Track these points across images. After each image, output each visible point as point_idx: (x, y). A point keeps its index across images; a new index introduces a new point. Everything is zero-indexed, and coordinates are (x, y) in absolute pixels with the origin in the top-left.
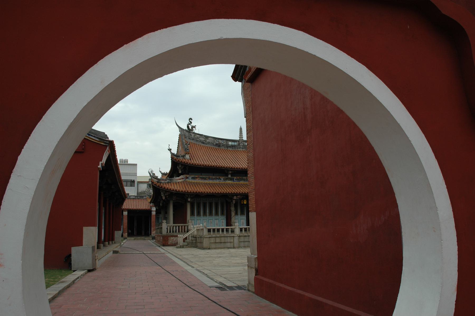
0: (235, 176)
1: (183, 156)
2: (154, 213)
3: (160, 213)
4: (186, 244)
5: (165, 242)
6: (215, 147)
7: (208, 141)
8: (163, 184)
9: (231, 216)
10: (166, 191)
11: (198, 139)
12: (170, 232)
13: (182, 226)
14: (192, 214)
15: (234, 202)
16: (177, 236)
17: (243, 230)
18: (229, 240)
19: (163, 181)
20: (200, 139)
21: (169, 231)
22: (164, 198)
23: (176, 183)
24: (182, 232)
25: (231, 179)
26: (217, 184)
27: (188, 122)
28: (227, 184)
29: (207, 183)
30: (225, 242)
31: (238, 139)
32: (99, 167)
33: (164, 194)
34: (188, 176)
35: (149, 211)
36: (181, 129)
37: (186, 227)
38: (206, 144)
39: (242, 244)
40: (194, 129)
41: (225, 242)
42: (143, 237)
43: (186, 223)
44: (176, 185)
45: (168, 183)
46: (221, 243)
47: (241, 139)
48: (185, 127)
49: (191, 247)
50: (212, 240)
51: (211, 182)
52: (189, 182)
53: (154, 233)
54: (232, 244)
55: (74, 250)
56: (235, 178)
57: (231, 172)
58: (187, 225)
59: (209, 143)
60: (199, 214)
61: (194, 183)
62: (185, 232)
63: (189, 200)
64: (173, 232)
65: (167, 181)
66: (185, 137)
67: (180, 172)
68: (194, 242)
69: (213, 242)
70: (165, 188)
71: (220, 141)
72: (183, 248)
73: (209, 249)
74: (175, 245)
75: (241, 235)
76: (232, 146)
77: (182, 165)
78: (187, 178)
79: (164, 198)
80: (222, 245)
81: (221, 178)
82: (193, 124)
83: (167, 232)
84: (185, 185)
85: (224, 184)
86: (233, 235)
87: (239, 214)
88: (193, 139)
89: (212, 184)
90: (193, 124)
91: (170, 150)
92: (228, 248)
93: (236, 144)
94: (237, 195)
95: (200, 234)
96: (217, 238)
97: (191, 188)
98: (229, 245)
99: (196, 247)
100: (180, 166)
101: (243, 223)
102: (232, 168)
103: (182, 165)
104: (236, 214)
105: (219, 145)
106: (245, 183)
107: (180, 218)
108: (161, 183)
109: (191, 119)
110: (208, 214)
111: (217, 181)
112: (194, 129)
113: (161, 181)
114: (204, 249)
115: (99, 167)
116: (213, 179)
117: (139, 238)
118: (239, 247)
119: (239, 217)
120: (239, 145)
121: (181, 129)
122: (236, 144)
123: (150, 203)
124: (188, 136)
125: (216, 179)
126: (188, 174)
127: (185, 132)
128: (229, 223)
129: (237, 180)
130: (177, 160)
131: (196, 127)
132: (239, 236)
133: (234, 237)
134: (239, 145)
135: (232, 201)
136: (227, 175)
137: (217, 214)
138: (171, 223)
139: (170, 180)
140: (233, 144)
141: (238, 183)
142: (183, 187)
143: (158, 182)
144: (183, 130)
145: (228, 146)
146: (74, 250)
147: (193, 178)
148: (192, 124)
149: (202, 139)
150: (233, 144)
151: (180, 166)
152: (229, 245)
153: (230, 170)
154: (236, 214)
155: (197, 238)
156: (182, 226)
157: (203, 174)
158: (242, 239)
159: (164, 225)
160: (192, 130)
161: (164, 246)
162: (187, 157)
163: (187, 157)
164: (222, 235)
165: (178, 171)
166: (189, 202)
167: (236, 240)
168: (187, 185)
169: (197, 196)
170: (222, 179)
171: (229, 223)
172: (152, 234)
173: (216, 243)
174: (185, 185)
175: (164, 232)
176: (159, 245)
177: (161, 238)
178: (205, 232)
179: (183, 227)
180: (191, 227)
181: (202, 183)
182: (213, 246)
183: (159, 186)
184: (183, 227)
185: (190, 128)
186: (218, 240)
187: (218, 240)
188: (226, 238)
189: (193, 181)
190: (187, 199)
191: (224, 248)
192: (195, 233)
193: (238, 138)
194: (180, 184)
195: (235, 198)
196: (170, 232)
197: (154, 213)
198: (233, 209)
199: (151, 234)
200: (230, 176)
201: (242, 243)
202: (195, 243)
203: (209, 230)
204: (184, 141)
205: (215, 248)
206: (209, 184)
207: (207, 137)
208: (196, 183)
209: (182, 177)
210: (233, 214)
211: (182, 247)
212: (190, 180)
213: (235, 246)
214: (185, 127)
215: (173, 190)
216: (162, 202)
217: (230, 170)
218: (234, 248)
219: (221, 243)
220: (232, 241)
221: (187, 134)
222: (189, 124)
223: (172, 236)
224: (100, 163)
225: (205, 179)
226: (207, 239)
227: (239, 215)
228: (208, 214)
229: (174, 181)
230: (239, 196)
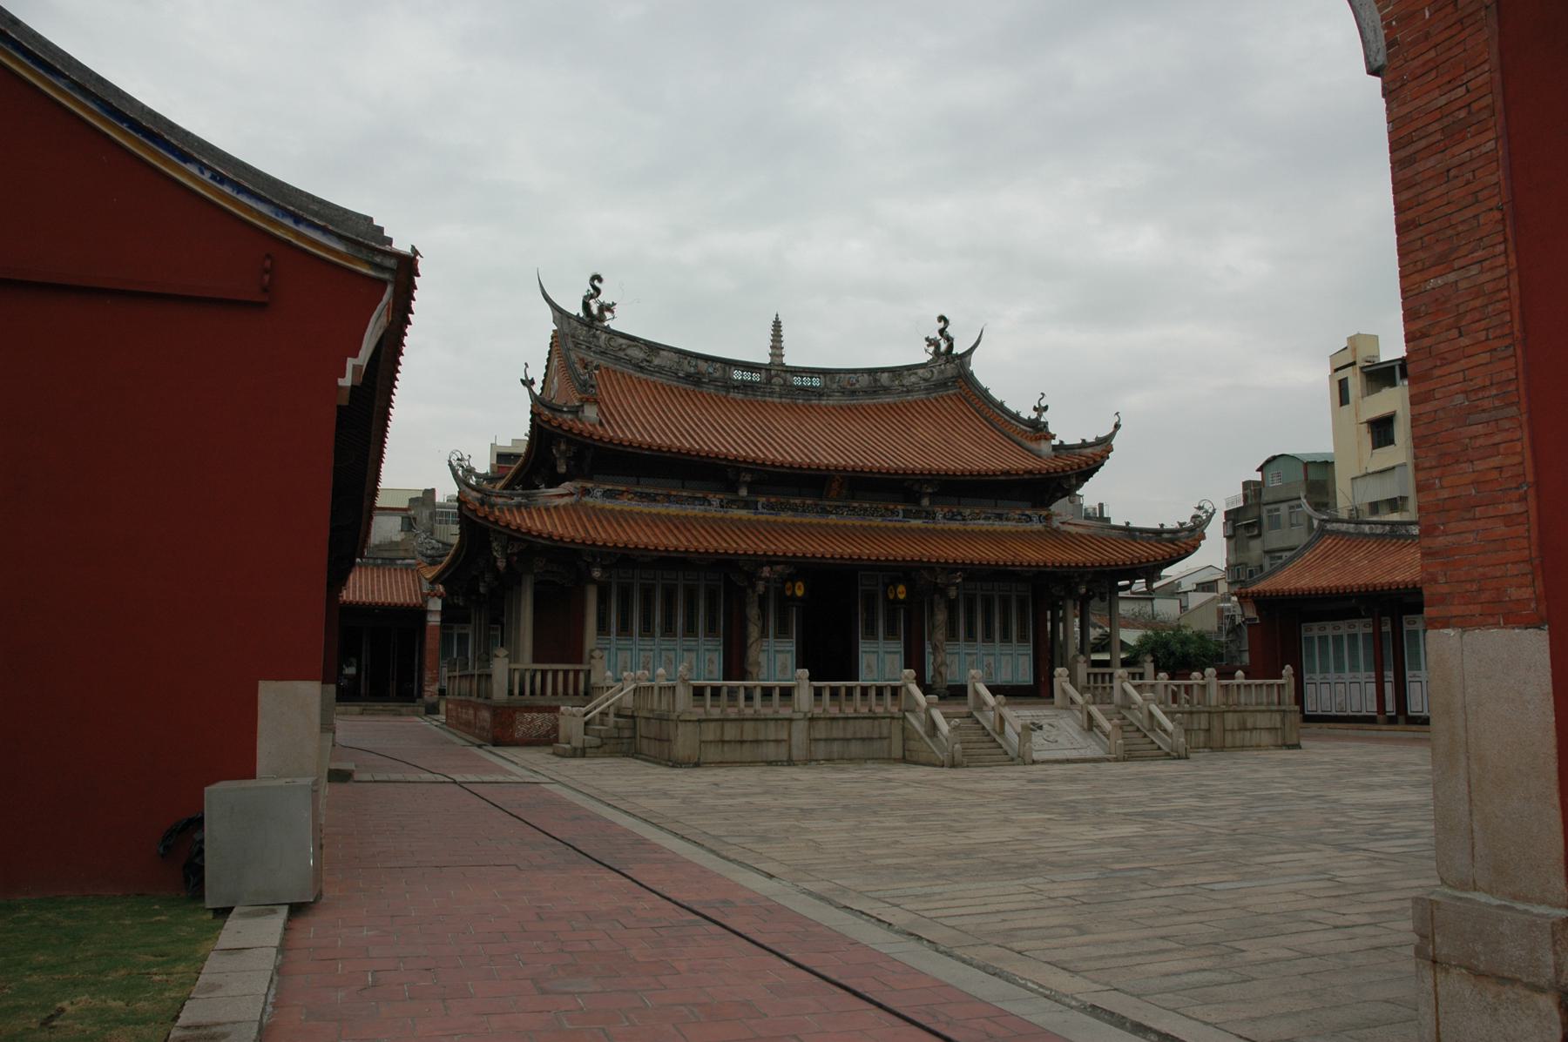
1: (576, 411)
2: (434, 620)
3: (467, 620)
4: (593, 741)
5: (501, 731)
6: (681, 385)
7: (656, 361)
8: (501, 510)
9: (744, 637)
10: (511, 539)
11: (621, 354)
12: (522, 693)
13: (566, 672)
14: (603, 628)
15: (761, 587)
16: (558, 708)
17: (873, 693)
18: (771, 732)
19: (500, 500)
20: (629, 352)
21: (516, 691)
22: (501, 564)
23: (547, 509)
24: (566, 692)
25: (746, 505)
26: (695, 518)
27: (586, 288)
28: (732, 520)
29: (658, 515)
30: (757, 741)
31: (766, 360)
32: (341, 382)
33: (504, 548)
34: (589, 485)
35: (419, 613)
36: (559, 313)
37: (582, 676)
38: (652, 373)
39: (821, 750)
40: (608, 315)
42: (393, 706)
43: (581, 662)
44: (550, 516)
45: (519, 506)
46: (742, 742)
47: (777, 360)
48: (576, 309)
49: (612, 754)
50: (711, 732)
51: (674, 510)
52: (593, 508)
53: (431, 690)
54: (783, 749)
55: (220, 797)
56: (762, 500)
57: (748, 478)
58: (585, 667)
59: (660, 370)
60: (625, 629)
61: (611, 511)
62: (576, 692)
63: (597, 574)
64: (533, 693)
65: (517, 500)
66: (577, 345)
67: (562, 469)
68: (627, 733)
69: (710, 737)
70: (507, 526)
71: (703, 366)
72: (583, 756)
73: (697, 765)
74: (547, 740)
75: (818, 711)
76: (745, 386)
77: (569, 442)
78: (586, 492)
79: (501, 564)
80: (747, 752)
82: (604, 298)
83: (511, 692)
84: (580, 518)
85: (721, 519)
86: (785, 712)
87: (771, 632)
88: (603, 353)
89: (677, 517)
90: (604, 298)
91: (528, 383)
92: (770, 763)
93: (756, 377)
94: (771, 560)
95: (659, 704)
96: (728, 725)
97: (606, 531)
98: (770, 751)
99: (634, 753)
100: (563, 447)
101: (784, 668)
102: (754, 462)
104: (764, 634)
105: (695, 379)
106: (797, 520)
107: (560, 642)
108: (492, 506)
109: (597, 278)
110: (658, 630)
111: (697, 510)
112: (608, 315)
113: (493, 499)
114: (676, 764)
115: (341, 382)
116: (679, 501)
117: (379, 706)
118: (809, 761)
119: (771, 642)
120: (769, 381)
121: (559, 313)
122: (756, 377)
123: (433, 582)
124: (584, 339)
125: (692, 500)
126: (589, 478)
127: (575, 324)
128: (736, 665)
129: (770, 507)
130: (555, 423)
131: (616, 309)
132: (812, 719)
133: (790, 720)
134: (769, 381)
135: (753, 586)
136: (732, 487)
137: (690, 630)
138: (526, 661)
139: (527, 497)
140: (747, 376)
141: (772, 518)
142: (574, 525)
143: (482, 503)
144: (569, 316)
145: (729, 386)
146: (220, 797)
147: (609, 494)
148: (601, 298)
149: (636, 353)
150: (747, 376)
151: (563, 447)
152: (770, 751)
153: (747, 470)
154: (764, 634)
155: (641, 724)
156: (566, 672)
157: (642, 480)
158: (821, 731)
159: (500, 667)
160: (601, 319)
161: (497, 742)
162: (591, 412)
163: (591, 412)
164: (749, 712)
165: (554, 467)
166: (594, 581)
167: (799, 732)
168: (590, 520)
169: (624, 558)
170: (716, 502)
171: (736, 665)
172: (426, 696)
173: (723, 742)
174: (580, 518)
175: (499, 692)
176: (478, 742)
177: (486, 715)
178: (683, 697)
179: (571, 675)
180: (601, 673)
181: (640, 513)
182: (712, 753)
183: (486, 518)
184: (571, 675)
185: (595, 310)
186: (731, 732)
187: (731, 732)
188: (761, 725)
189: (609, 504)
190: (590, 572)
191: (752, 763)
192: (628, 701)
193: (765, 359)
194: (556, 513)
195: (766, 571)
196: (522, 693)
197: (434, 620)
198: (753, 612)
199: (420, 695)
200: (743, 492)
201: (822, 744)
202: (633, 737)
203: (698, 692)
204: (573, 356)
205: (721, 764)
206: (668, 516)
207: (654, 348)
208: (621, 512)
209: (567, 487)
210: (754, 631)
211: (581, 753)
212: (596, 501)
213: (796, 754)
214: (576, 309)
215: (540, 536)
216: (488, 577)
217: (747, 470)
218: (790, 762)
219: (742, 742)
220: (785, 737)
221: (582, 332)
222: (592, 297)
223: (530, 709)
224: (350, 362)
225: (652, 499)
226: (690, 726)
227: (771, 639)
228: (658, 630)
229: (541, 501)
230: (779, 568)
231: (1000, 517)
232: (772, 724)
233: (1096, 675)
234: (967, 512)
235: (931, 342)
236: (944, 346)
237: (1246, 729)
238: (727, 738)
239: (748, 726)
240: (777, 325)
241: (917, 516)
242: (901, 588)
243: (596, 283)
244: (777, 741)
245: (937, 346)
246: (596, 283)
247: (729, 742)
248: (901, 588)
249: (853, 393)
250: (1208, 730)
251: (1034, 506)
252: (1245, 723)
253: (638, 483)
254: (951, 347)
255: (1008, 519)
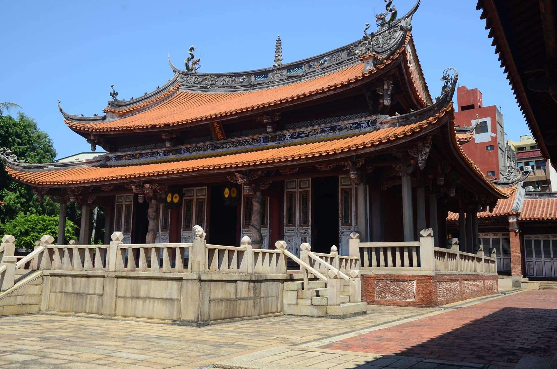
0: (183, 144)
40: (197, 66)
77: (95, 135)
81: (159, 150)
82: (195, 59)
90: (195, 59)
103: (95, 135)
109: (192, 49)
111: (154, 159)
116: (146, 155)
125: (152, 154)
129: (187, 150)
189: (116, 163)
193: (269, 64)
230: (147, 186)
231: (333, 129)
233: (370, 250)
234: (307, 130)
235: (381, 18)
236: (388, 18)
237: (139, 298)
240: (279, 41)
241: (273, 139)
242: (227, 190)
243: (192, 52)
245: (383, 19)
246: (192, 52)
248: (227, 190)
249: (323, 69)
250: (102, 295)
251: (370, 115)
252: (138, 290)
253: (136, 150)
254: (394, 15)
255: (340, 130)
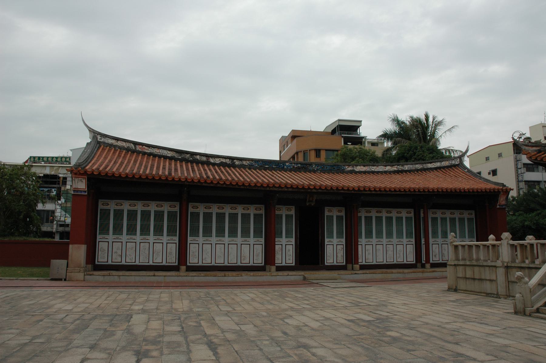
18: (487, 274)
30: (481, 280)
41: (481, 280)
46: (474, 279)
50: (460, 272)
92: (488, 295)
96: (468, 268)
132: (507, 267)
133: (495, 267)
152: (488, 287)
182: (462, 285)
218: (498, 296)
220: (494, 278)
232: (487, 268)
238: (467, 276)
239: (476, 269)
244: (491, 280)
247: (469, 278)
